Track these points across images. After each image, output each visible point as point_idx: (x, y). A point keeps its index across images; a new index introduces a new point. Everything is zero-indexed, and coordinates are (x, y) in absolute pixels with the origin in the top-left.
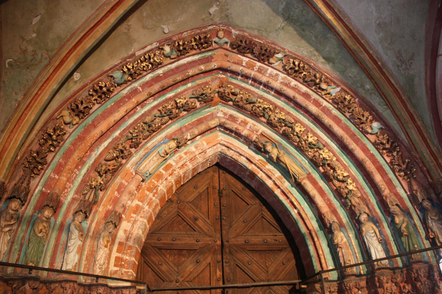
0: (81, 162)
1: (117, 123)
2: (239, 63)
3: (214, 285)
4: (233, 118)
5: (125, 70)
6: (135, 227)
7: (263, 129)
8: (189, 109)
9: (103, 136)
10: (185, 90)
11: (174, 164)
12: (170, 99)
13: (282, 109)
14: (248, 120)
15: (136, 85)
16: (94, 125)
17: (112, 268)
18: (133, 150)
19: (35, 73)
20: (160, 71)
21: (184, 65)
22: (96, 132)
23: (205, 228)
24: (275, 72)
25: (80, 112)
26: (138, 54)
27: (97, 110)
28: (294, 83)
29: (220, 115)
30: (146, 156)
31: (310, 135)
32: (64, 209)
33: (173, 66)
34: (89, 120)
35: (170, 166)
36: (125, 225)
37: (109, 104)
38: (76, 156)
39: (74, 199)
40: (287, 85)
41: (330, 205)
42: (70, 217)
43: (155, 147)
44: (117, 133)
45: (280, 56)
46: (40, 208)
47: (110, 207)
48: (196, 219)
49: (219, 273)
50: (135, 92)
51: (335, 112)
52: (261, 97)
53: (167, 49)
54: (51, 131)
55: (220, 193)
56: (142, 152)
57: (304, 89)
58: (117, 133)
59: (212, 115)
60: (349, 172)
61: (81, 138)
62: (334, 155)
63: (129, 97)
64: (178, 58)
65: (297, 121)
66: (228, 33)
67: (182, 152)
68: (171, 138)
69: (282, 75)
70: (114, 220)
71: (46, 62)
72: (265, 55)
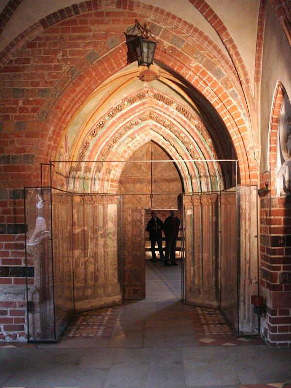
0: (96, 153)
1: (108, 137)
2: (158, 104)
3: (147, 193)
4: (156, 126)
5: (109, 115)
6: (116, 173)
7: (168, 131)
8: (136, 124)
9: (103, 142)
10: (135, 117)
11: (131, 146)
12: (128, 122)
13: (176, 126)
14: (162, 127)
15: (114, 119)
16: (99, 139)
17: (109, 188)
18: (114, 144)
19: (79, 127)
20: (123, 112)
21: (133, 107)
22: (101, 141)
23: (144, 169)
24: (173, 110)
25: (93, 134)
26: (115, 107)
27: (100, 132)
28: (181, 115)
29: (150, 124)
30: (120, 145)
31: (186, 138)
32: (92, 170)
33: (129, 108)
34: (97, 137)
35: (129, 147)
36: (113, 172)
37: (104, 129)
38: (94, 152)
39: (95, 167)
40: (178, 117)
41: (192, 167)
42: (95, 173)
43: (123, 141)
44: (108, 139)
45: (175, 104)
46: (86, 172)
47: (107, 167)
48: (141, 166)
49: (150, 188)
50: (114, 123)
51: (196, 131)
52: (168, 120)
53: (126, 103)
54: (85, 145)
55: (152, 153)
56: (117, 144)
57: (185, 119)
58: (108, 139)
59: (147, 124)
60: (199, 155)
61: (96, 145)
62: (195, 148)
63: (112, 125)
64: (131, 105)
65: (182, 132)
66: (152, 92)
67: (134, 141)
68: (129, 136)
69: (176, 112)
70: (108, 171)
71: (81, 122)
72: (169, 103)
